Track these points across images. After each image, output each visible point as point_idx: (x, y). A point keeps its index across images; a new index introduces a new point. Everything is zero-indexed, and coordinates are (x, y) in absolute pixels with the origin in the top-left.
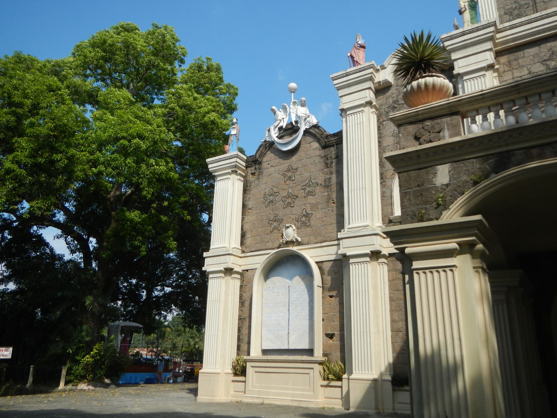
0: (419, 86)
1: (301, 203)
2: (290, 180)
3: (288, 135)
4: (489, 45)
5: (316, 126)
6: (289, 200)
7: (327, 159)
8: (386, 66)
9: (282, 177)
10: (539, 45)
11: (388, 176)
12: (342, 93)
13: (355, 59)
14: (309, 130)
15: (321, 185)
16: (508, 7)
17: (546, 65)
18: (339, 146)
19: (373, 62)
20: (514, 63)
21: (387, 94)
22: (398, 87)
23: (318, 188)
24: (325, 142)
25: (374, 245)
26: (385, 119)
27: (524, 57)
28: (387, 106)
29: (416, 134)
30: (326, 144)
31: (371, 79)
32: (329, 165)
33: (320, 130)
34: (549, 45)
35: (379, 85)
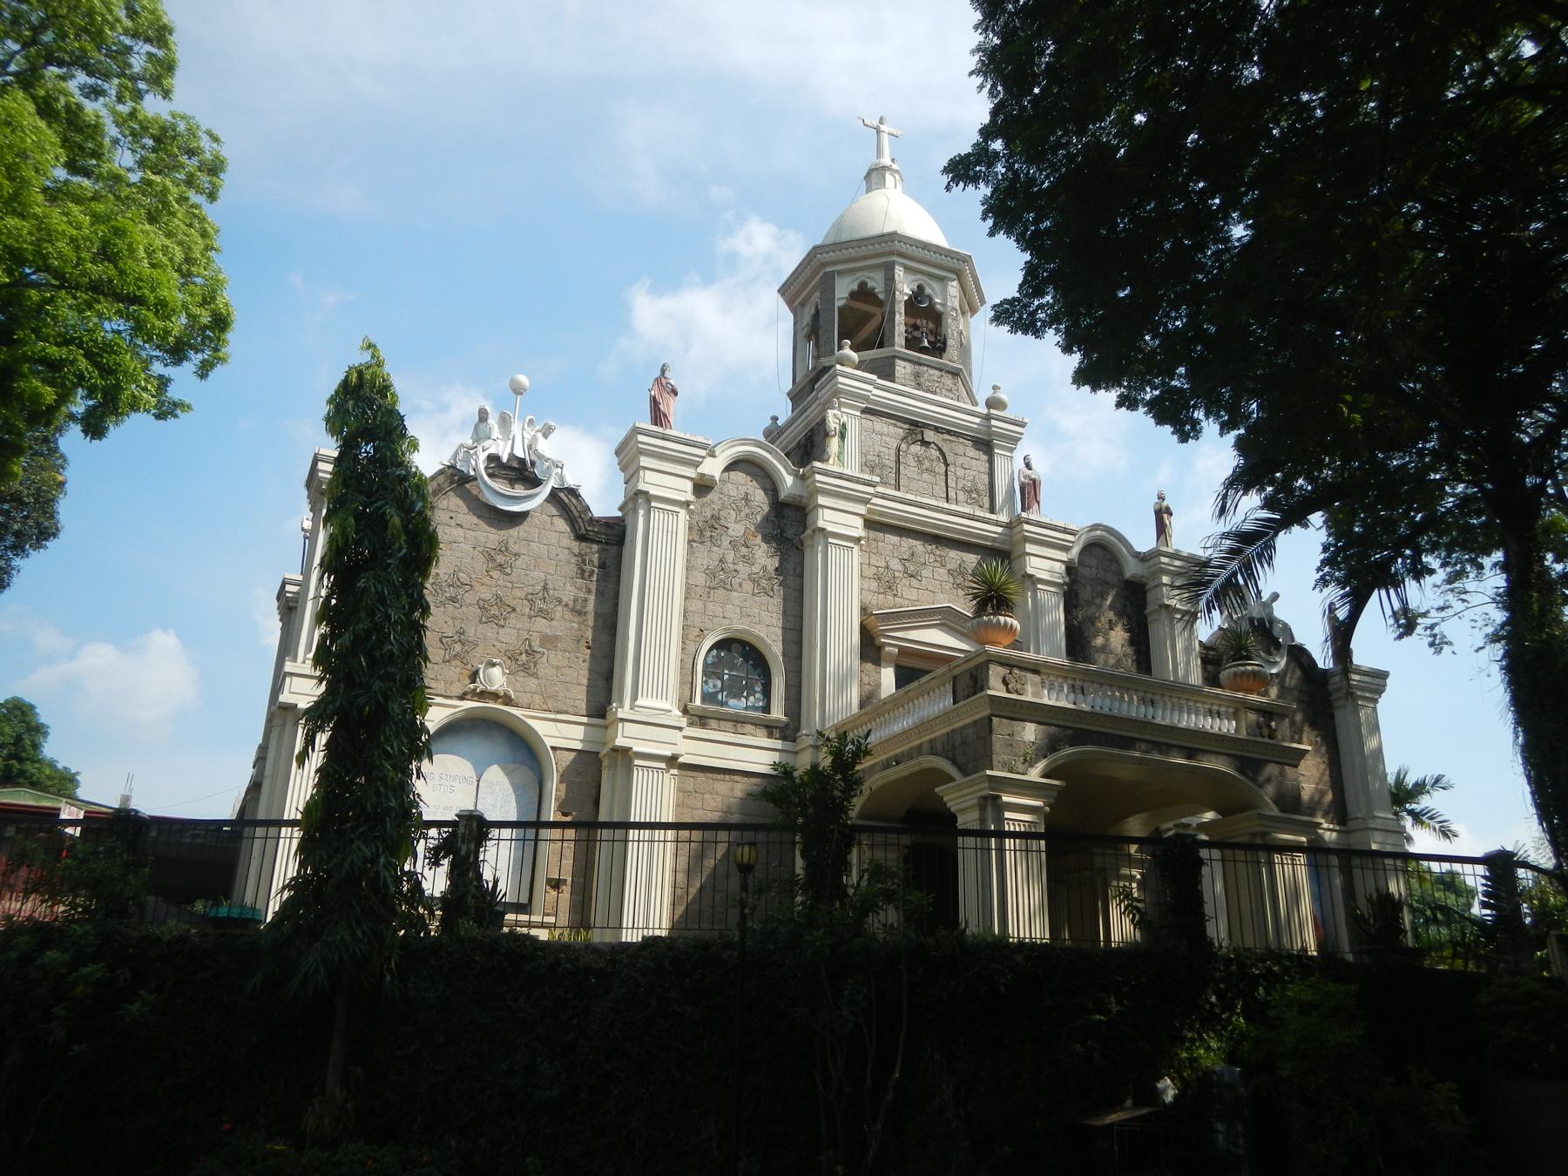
0: (1005, 622)
1: (519, 626)
2: (501, 571)
3: (505, 479)
4: (862, 509)
5: (573, 492)
6: (494, 611)
7: (584, 562)
8: (717, 454)
9: (481, 559)
10: (901, 536)
11: (691, 637)
12: (645, 461)
13: (662, 409)
14: (556, 491)
15: (566, 605)
16: (869, 457)
17: (904, 565)
18: (608, 547)
19: (709, 442)
20: (873, 544)
21: (704, 500)
22: (722, 496)
23: (560, 608)
24: (586, 530)
25: (676, 744)
26: (696, 538)
27: (883, 541)
28: (704, 519)
29: (1004, 678)
30: (587, 534)
31: (696, 465)
32: (586, 575)
33: (581, 503)
34: (910, 540)
35: (700, 479)
